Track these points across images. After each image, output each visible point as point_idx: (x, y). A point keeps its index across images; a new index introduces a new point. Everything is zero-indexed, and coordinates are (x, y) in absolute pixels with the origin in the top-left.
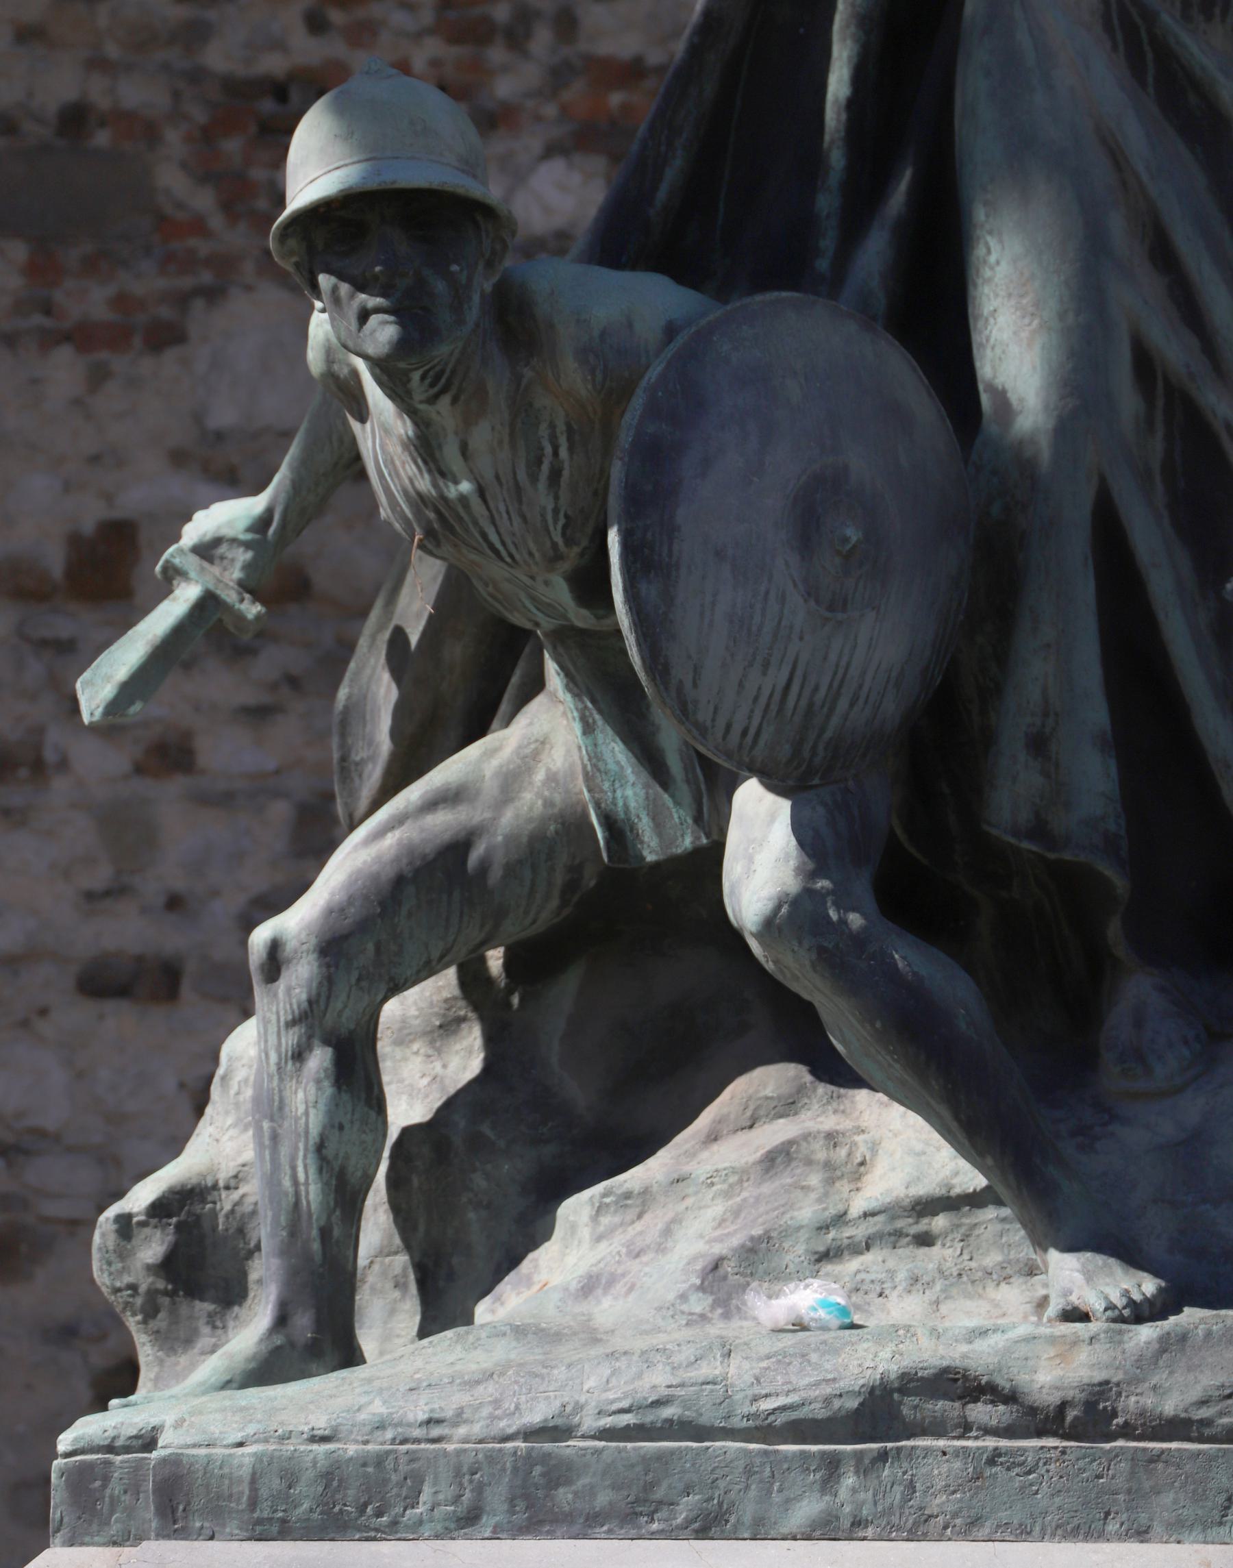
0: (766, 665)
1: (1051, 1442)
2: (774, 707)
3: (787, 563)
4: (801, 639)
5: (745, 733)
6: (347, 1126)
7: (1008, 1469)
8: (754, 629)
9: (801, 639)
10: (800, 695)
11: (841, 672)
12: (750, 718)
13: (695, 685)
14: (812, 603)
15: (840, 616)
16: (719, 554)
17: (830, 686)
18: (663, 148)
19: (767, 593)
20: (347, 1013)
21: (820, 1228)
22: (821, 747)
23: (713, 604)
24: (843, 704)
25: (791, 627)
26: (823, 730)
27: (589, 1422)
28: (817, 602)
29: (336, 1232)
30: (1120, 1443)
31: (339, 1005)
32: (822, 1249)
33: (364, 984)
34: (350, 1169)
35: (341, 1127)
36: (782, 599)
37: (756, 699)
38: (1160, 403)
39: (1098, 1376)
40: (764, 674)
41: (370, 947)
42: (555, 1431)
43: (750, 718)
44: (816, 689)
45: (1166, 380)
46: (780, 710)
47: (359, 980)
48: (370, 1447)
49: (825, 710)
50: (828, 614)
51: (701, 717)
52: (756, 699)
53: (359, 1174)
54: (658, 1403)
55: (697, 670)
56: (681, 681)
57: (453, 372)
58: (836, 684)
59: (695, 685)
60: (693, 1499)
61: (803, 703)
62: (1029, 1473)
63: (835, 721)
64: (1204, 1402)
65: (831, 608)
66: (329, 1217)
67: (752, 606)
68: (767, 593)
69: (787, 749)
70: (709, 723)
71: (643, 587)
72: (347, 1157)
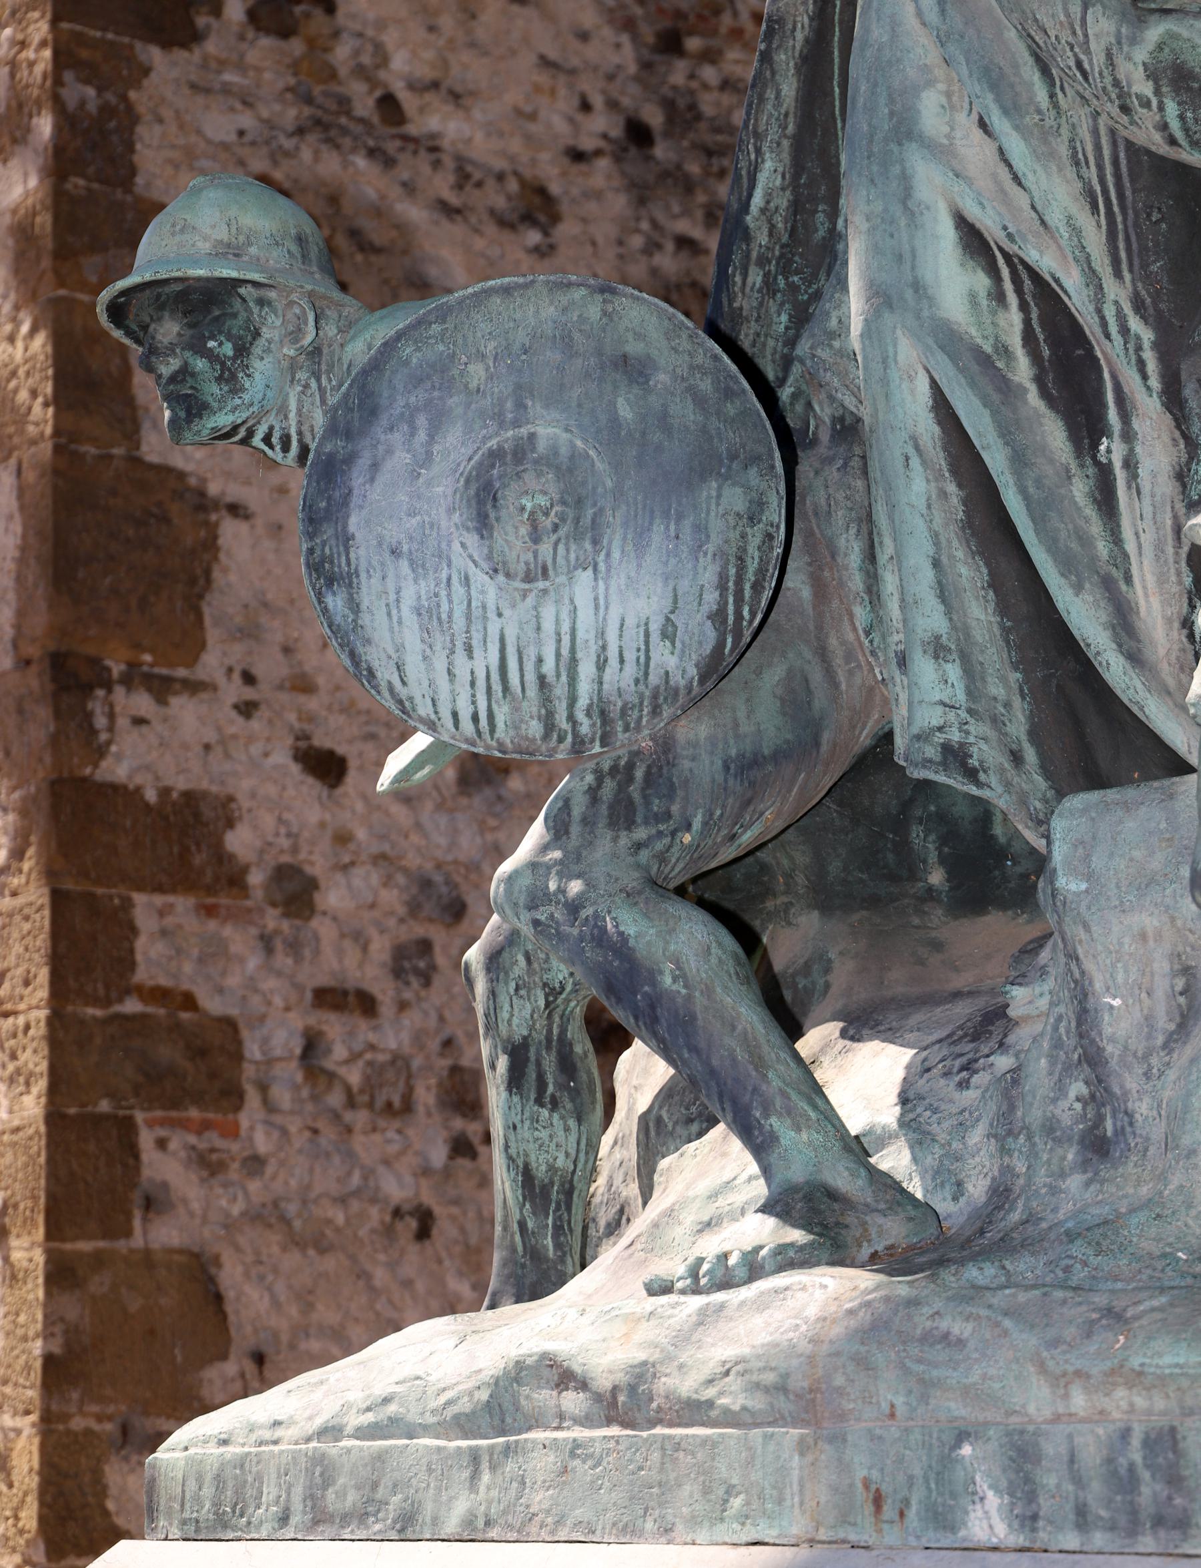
0: (469, 650)
1: (615, 1431)
2: (497, 687)
3: (463, 545)
4: (500, 615)
5: (475, 718)
6: (519, 1126)
7: (584, 1462)
8: (444, 616)
9: (500, 615)
10: (521, 670)
11: (566, 640)
12: (474, 703)
13: (404, 683)
14: (501, 578)
15: (541, 584)
16: (395, 552)
17: (558, 655)
18: (753, 156)
19: (449, 579)
20: (515, 1021)
21: (710, 1197)
22: (580, 716)
23: (398, 601)
24: (586, 670)
25: (484, 607)
26: (572, 700)
27: (355, 1420)
28: (508, 575)
29: (530, 1224)
30: (659, 1430)
31: (506, 1015)
32: (706, 1218)
33: (522, 992)
34: (534, 1165)
35: (515, 1127)
36: (466, 581)
37: (473, 684)
38: (1005, 272)
39: (641, 1356)
40: (471, 657)
41: (521, 958)
42: (330, 1432)
43: (474, 703)
44: (540, 660)
45: (1001, 249)
46: (506, 689)
47: (517, 989)
48: (230, 1449)
49: (564, 678)
50: (527, 586)
51: (422, 711)
52: (473, 684)
53: (543, 1168)
54: (386, 1400)
55: (399, 667)
56: (389, 682)
57: (300, 433)
58: (565, 652)
59: (404, 683)
60: (396, 1499)
61: (531, 677)
62: (599, 1464)
63: (585, 689)
64: (710, 1382)
65: (528, 578)
66: (521, 1210)
67: (436, 595)
68: (449, 579)
69: (535, 728)
70: (433, 717)
71: (329, 600)
72: (526, 1155)
